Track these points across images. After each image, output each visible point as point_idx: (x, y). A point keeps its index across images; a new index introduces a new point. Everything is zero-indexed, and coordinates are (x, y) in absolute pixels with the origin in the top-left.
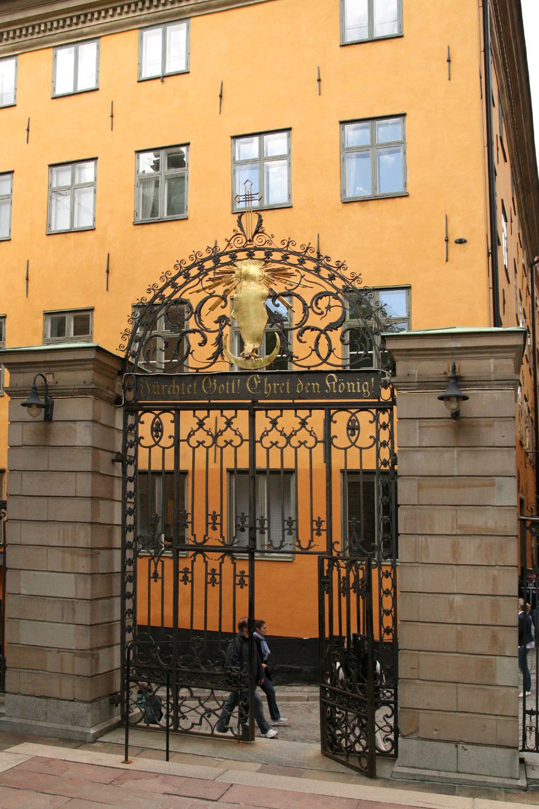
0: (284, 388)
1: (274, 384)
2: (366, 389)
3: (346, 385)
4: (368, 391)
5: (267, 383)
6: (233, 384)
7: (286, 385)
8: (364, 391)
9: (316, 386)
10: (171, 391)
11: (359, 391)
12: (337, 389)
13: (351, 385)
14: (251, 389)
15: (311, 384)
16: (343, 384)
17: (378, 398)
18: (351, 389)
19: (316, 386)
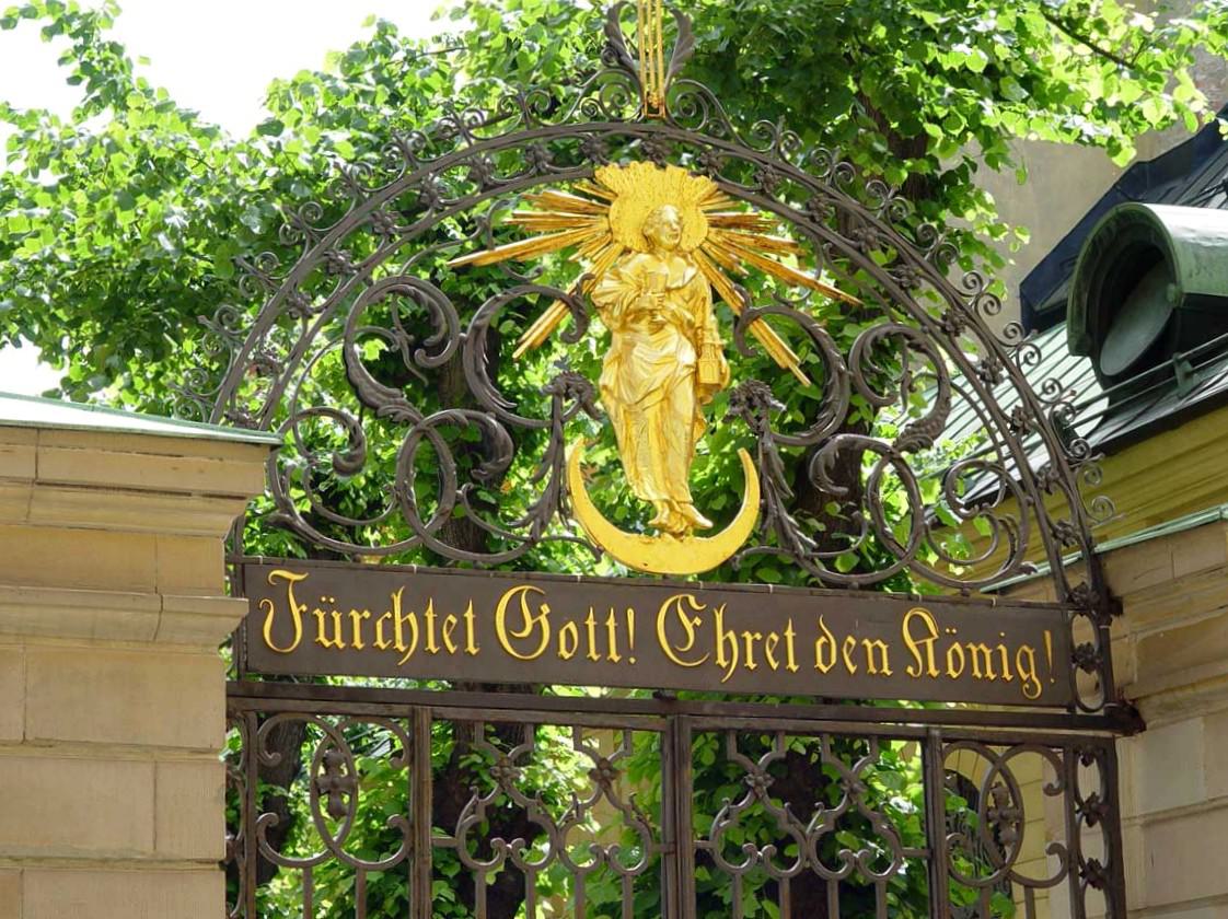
0: (781, 653)
1: (747, 635)
2: (1027, 670)
3: (968, 653)
4: (1034, 678)
5: (725, 632)
6: (611, 623)
7: (783, 639)
8: (1024, 677)
9: (877, 650)
10: (389, 633)
11: (1007, 675)
12: (941, 663)
13: (981, 654)
14: (674, 650)
15: (859, 640)
16: (957, 646)
17: (1071, 708)
18: (982, 669)
19: (877, 650)
